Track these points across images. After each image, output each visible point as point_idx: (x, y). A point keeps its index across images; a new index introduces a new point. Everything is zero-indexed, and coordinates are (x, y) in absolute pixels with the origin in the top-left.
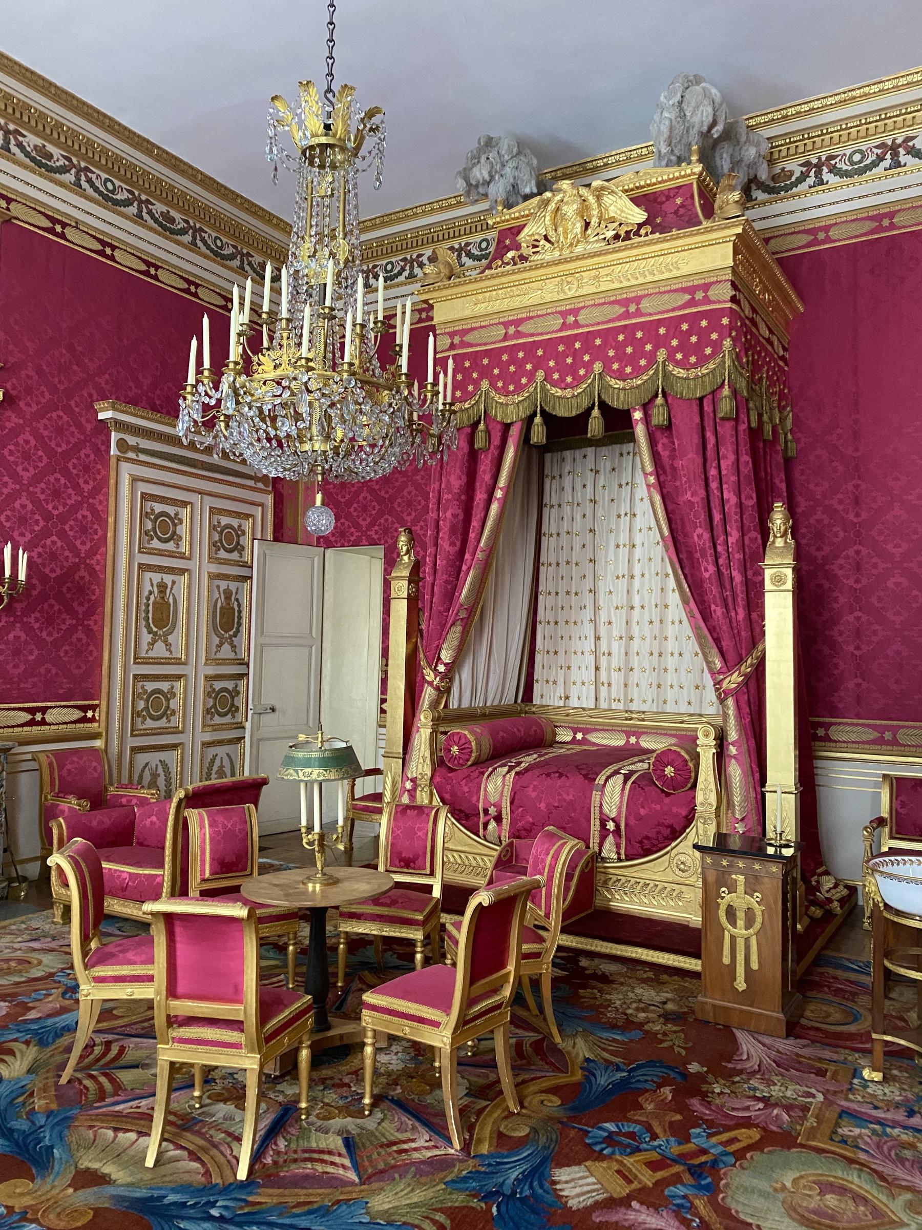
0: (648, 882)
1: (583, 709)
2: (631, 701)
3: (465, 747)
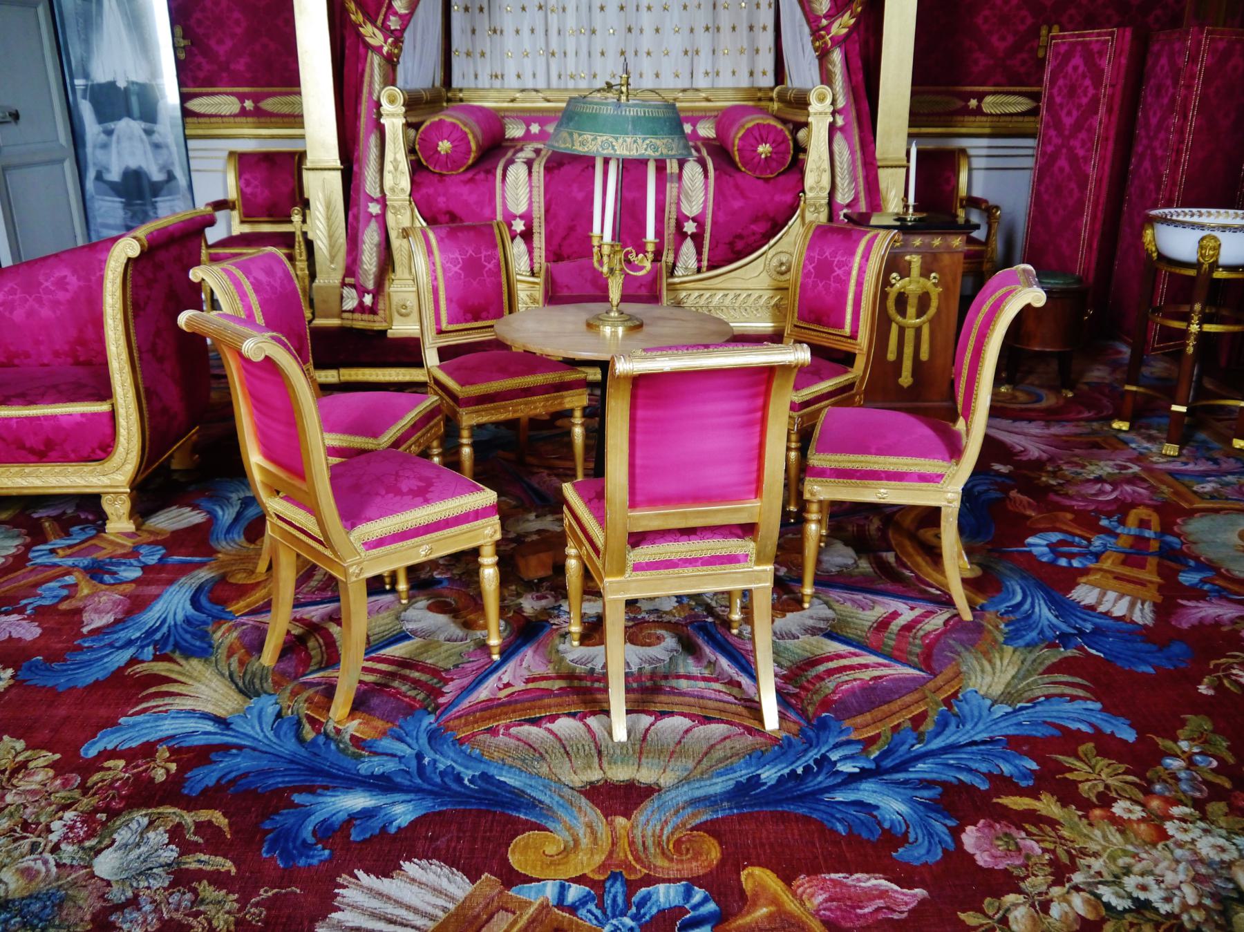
0: (738, 292)
1: (536, 91)
2: (595, 76)
3: (460, 140)
